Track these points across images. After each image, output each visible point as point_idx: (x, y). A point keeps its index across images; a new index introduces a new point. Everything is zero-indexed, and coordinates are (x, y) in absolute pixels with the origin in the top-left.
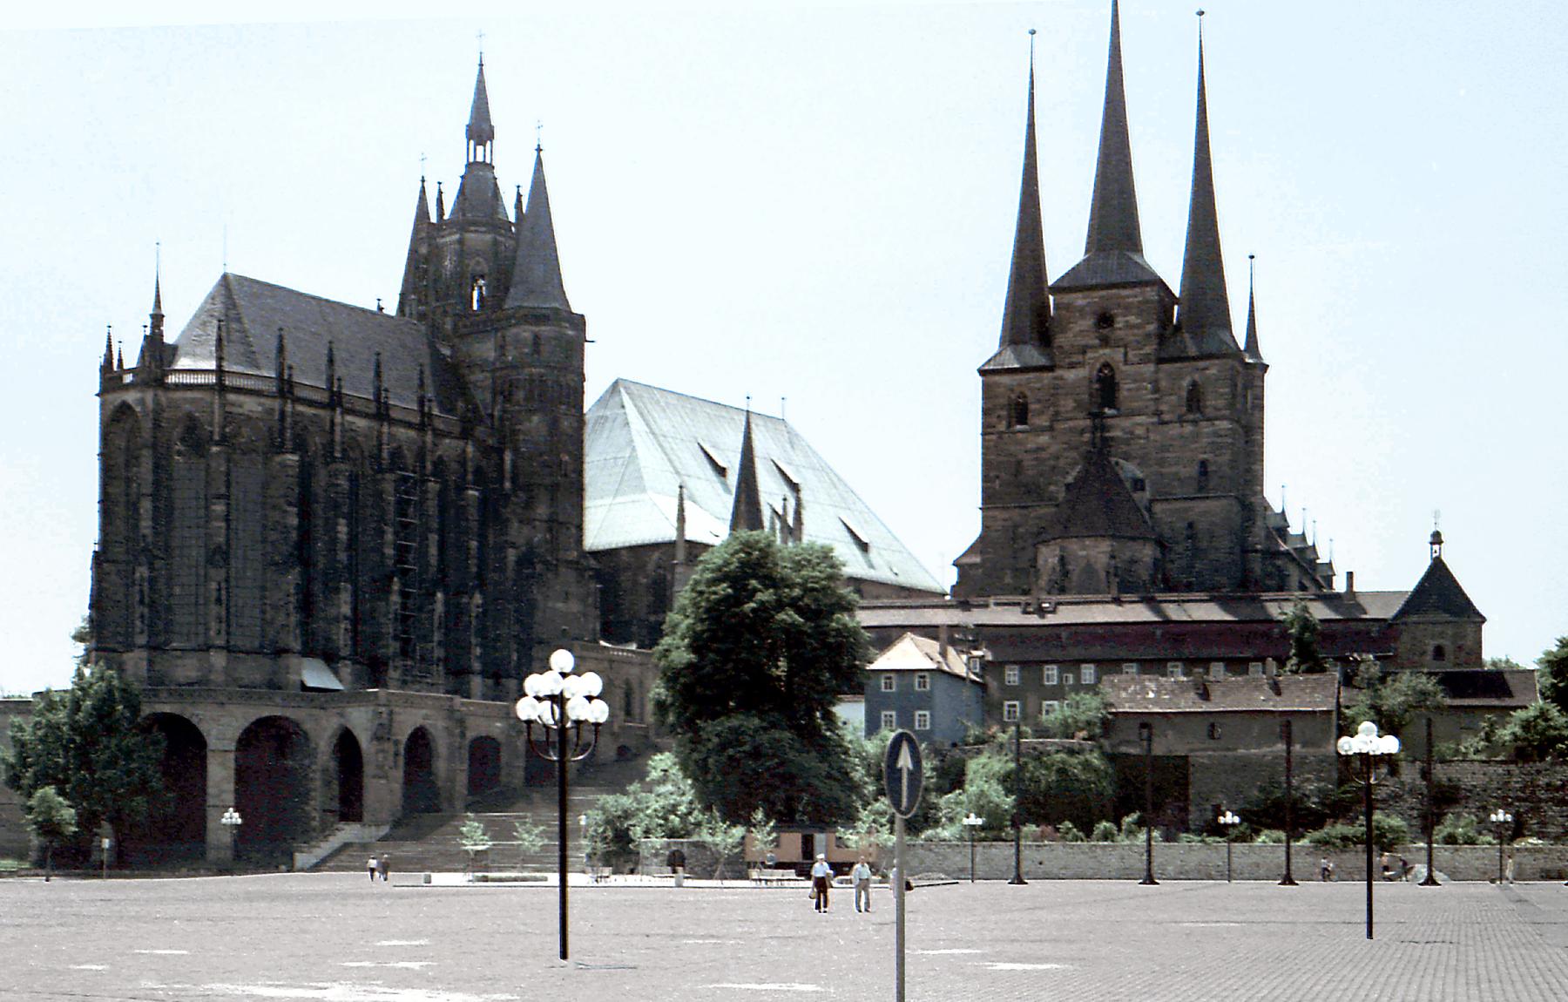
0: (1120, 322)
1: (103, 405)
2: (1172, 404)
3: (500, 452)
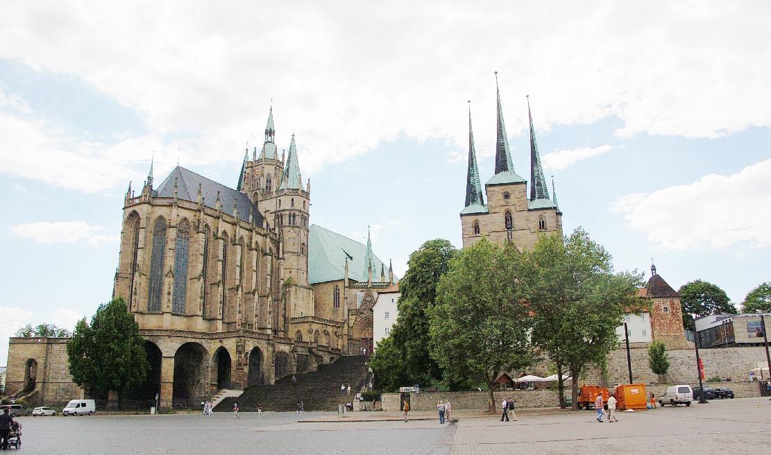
0: (512, 197)
1: (125, 214)
2: (535, 225)
3: (279, 242)
